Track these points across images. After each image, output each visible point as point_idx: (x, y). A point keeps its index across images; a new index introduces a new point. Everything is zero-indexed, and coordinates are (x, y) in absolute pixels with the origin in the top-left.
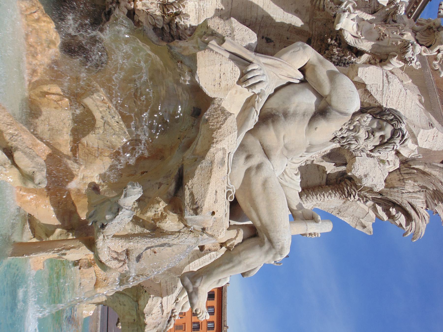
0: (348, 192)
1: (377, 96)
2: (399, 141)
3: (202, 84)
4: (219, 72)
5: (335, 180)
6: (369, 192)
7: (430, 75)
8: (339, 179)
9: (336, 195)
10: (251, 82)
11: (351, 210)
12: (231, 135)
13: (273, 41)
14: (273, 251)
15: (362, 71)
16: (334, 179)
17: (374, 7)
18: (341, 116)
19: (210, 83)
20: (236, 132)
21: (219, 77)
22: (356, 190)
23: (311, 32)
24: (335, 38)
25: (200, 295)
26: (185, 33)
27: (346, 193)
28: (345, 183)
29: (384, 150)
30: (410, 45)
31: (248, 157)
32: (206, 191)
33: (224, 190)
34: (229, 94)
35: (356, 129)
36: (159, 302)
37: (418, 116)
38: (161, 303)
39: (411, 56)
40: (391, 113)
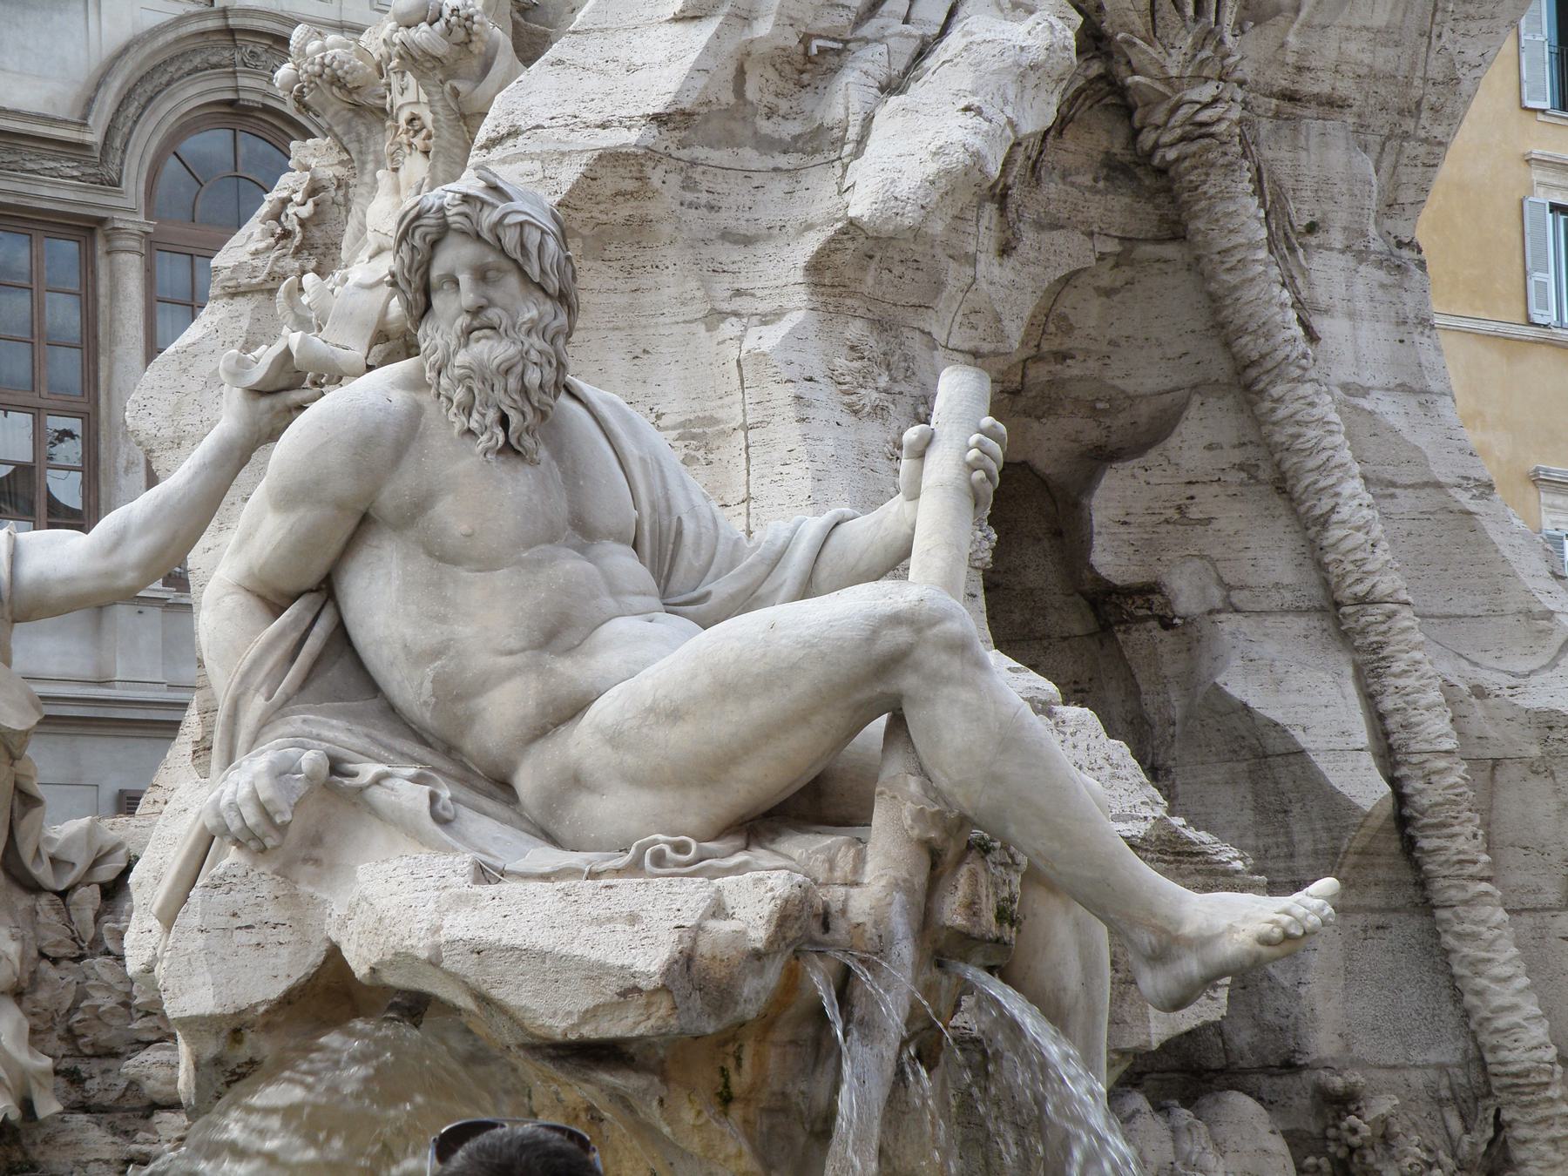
0: (1183, 139)
1: (562, 178)
2: (487, 211)
3: (276, 990)
6: (1166, 41)
16: (1157, 207)
17: (341, 163)
19: (273, 961)
22: (1165, 107)
25: (1205, 925)
27: (1193, 147)
31: (575, 781)
32: (579, 963)
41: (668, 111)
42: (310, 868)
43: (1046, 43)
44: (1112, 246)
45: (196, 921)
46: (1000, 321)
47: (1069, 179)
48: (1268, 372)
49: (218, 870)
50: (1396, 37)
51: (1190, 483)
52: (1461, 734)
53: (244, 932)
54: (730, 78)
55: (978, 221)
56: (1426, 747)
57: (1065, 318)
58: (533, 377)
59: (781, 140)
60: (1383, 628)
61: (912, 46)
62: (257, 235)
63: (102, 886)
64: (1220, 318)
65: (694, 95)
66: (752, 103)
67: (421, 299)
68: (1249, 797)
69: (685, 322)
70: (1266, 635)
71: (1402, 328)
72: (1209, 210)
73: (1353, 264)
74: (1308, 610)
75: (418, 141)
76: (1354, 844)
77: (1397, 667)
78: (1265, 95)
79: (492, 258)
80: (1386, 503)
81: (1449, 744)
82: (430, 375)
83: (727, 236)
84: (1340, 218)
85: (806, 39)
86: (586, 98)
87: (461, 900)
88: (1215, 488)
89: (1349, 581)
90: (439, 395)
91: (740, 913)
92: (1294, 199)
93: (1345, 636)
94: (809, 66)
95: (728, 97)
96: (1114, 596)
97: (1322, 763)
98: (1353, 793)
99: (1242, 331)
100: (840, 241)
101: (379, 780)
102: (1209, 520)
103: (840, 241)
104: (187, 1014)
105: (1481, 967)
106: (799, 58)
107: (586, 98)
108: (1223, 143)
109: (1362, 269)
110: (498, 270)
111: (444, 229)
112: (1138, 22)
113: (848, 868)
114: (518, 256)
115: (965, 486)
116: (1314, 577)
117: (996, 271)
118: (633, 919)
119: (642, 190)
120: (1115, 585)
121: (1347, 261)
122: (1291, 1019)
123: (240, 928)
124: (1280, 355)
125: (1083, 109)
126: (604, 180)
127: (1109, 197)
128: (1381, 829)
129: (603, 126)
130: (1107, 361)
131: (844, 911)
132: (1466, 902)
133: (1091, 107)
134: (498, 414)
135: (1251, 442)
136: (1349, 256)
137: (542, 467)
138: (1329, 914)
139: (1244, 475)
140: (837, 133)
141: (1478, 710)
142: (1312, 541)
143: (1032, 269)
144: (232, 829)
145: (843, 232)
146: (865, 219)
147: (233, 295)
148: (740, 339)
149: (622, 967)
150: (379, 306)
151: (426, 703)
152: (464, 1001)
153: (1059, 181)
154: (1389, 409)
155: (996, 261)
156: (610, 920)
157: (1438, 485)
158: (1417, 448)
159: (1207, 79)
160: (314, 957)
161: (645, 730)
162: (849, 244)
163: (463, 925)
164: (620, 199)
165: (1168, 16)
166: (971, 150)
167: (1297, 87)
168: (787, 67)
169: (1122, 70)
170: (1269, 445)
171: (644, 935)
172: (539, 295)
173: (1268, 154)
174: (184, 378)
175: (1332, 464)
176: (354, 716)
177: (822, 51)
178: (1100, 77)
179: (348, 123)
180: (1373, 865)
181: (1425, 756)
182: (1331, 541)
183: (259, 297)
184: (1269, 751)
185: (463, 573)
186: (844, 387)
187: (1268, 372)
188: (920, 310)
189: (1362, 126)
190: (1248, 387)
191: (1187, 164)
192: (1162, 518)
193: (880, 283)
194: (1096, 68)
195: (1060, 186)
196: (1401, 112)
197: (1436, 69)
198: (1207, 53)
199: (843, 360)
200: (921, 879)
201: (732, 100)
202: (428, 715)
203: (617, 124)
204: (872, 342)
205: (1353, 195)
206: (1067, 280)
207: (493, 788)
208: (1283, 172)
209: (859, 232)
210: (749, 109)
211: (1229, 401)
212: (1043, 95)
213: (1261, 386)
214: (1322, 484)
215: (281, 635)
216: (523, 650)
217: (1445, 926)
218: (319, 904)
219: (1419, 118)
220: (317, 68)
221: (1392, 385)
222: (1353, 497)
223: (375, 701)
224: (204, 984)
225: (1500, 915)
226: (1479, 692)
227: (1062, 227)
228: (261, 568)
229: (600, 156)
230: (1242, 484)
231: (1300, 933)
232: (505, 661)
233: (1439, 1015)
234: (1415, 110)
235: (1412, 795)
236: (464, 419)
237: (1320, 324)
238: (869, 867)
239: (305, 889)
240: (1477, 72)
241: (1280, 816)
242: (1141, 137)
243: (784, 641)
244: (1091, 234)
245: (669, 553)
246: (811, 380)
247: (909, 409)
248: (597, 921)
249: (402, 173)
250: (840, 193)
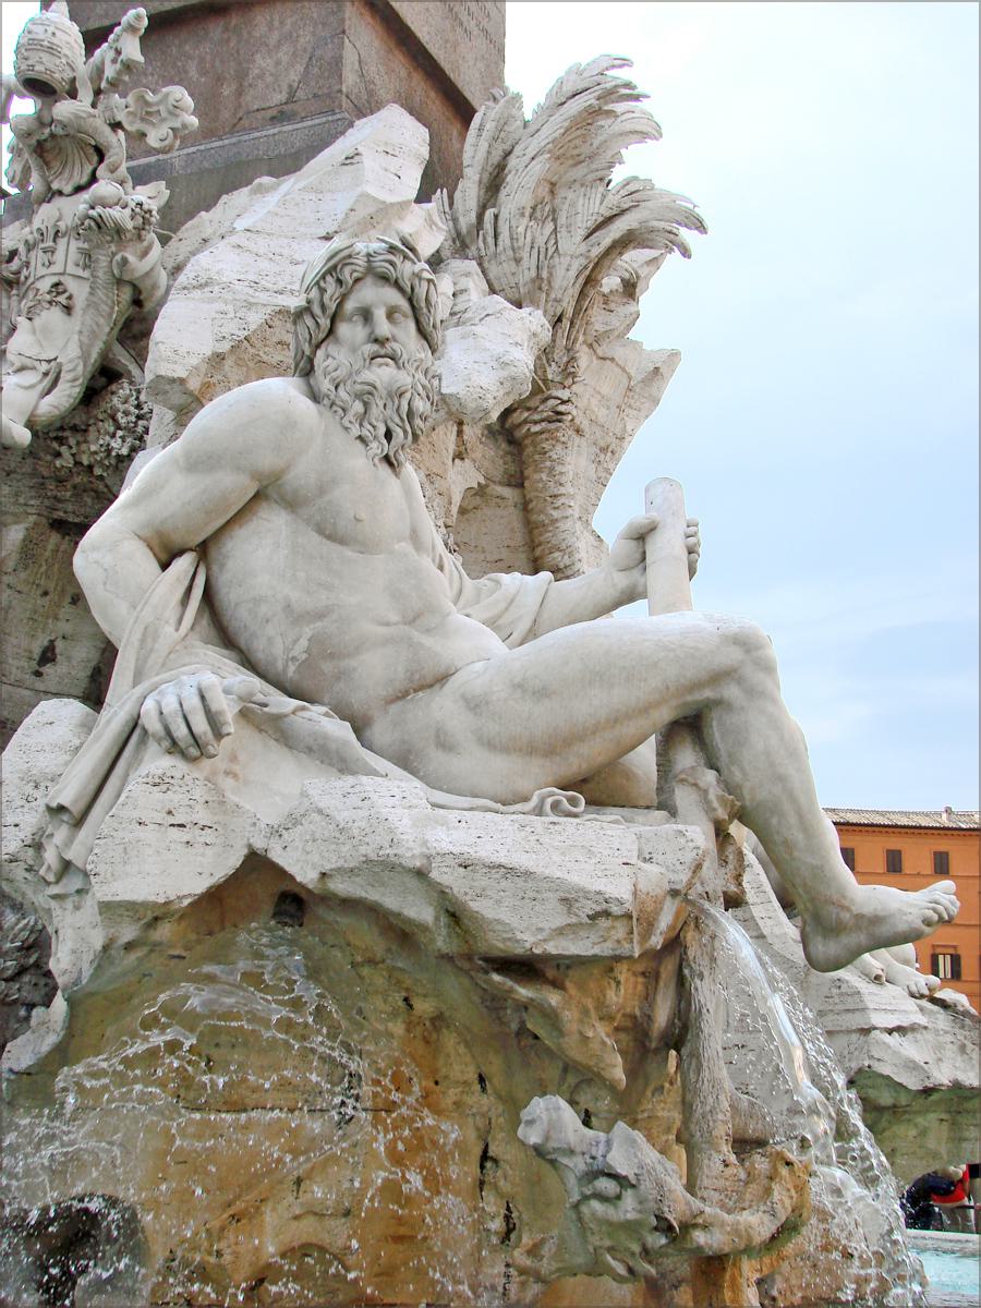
2: (408, 264)
3: (200, 886)
4: (163, 829)
7: (188, 154)
10: (201, 725)
11: (601, 414)
12: (374, 797)
13: (52, 642)
14: (749, 671)
15: (169, 366)
19: (200, 858)
20: (364, 779)
23: (32, 519)
24: (55, 445)
25: (879, 907)
26: (13, 929)
28: (520, 425)
29: (432, 311)
30: (92, 212)
32: (554, 884)
33: (551, 826)
34: (236, 799)
35: (366, 396)
36: (886, 1037)
37: (320, 196)
38: (890, 1031)
39: (128, 211)
40: (317, 283)
53: (176, 829)
67: (325, 322)
72: (552, 469)
75: (62, 299)
79: (404, 304)
104: (118, 899)
149: (599, 893)
160: (234, 861)
171: (604, 867)
185: (348, 553)
191: (543, 436)
218: (244, 813)
232: (382, 630)
239: (232, 797)
243: (647, 644)
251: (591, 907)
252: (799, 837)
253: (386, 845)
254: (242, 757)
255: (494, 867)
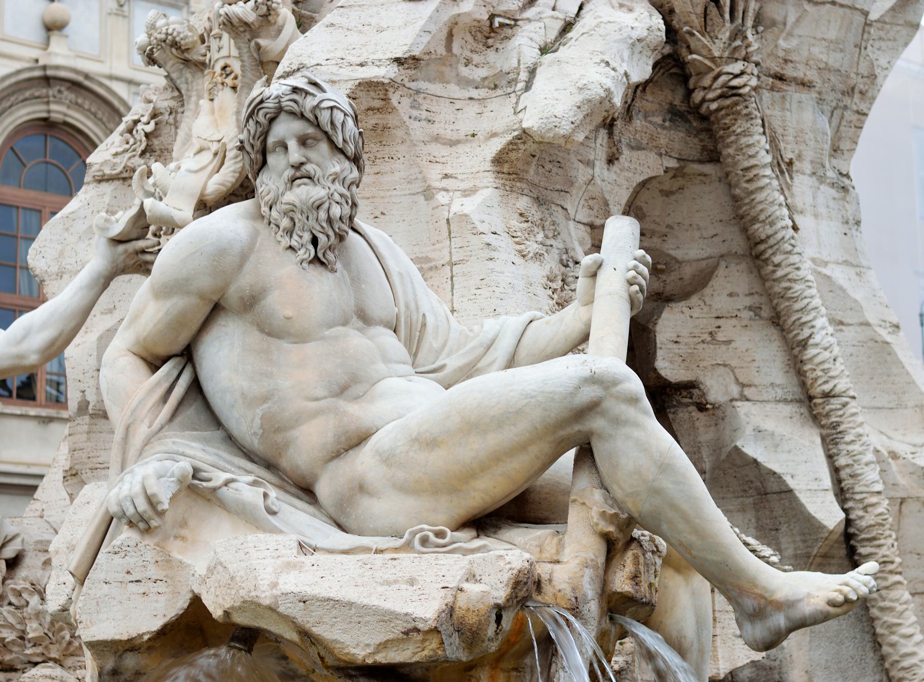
0: (722, 96)
2: (309, 98)
3: (156, 625)
4: (124, 585)
5: (703, 136)
6: (712, 34)
8: (695, 124)
9: (739, 130)
16: (701, 140)
17: (173, 98)
18: (253, 258)
21: (138, 583)
27: (728, 102)
31: (362, 488)
34: (180, 557)
41: (405, 56)
42: (178, 543)
43: (647, 26)
44: (673, 164)
45: (102, 576)
46: (608, 205)
47: (649, 119)
48: (771, 247)
49: (117, 542)
50: (841, 46)
51: (718, 317)
52: (884, 483)
53: (134, 584)
54: (444, 38)
55: (596, 140)
56: (865, 489)
57: (641, 209)
58: (336, 211)
59: (474, 80)
60: (840, 413)
61: (559, 25)
62: (117, 143)
63: (7, 561)
64: (741, 212)
65: (422, 47)
66: (456, 56)
67: (259, 157)
68: (753, 520)
69: (410, 194)
70: (767, 416)
71: (845, 226)
72: (735, 142)
73: (817, 184)
74: (791, 401)
75: (229, 81)
76: (821, 550)
77: (848, 438)
78: (766, 75)
79: (311, 130)
80: (839, 335)
81: (879, 487)
82: (264, 209)
83: (437, 139)
84: (809, 155)
85: (492, 17)
86: (350, 48)
87: (290, 566)
88: (734, 321)
89: (820, 382)
90: (270, 223)
91: (485, 578)
92: (783, 141)
93: (815, 418)
94: (492, 35)
95: (442, 51)
96: (668, 390)
97: (803, 498)
98: (822, 518)
99: (755, 220)
100: (516, 144)
101: (227, 483)
102: (729, 342)
103: (516, 144)
105: (894, 629)
106: (487, 29)
107: (350, 48)
108: (745, 100)
109: (822, 187)
110: (315, 139)
111: (280, 110)
112: (696, 21)
113: (554, 551)
114: (328, 128)
115: (626, 296)
116: (795, 380)
117: (606, 173)
118: (412, 582)
119: (386, 107)
120: (670, 382)
121: (813, 181)
122: (777, 663)
123: (132, 582)
124: (779, 236)
125: (659, 74)
126: (361, 99)
127: (672, 132)
128: (837, 541)
129: (362, 65)
130: (665, 238)
131: (550, 580)
132: (887, 588)
133: (663, 74)
134: (311, 237)
135: (757, 293)
136: (814, 178)
137: (338, 274)
138: (874, 586)
139: (752, 313)
140: (512, 76)
141: (894, 465)
142: (796, 357)
143: (626, 174)
144: (128, 514)
145: (519, 138)
146: (535, 129)
147: (100, 181)
148: (449, 205)
149: (406, 614)
150: (201, 185)
151: (255, 434)
152: (291, 635)
153: (643, 120)
154: (839, 274)
155: (606, 166)
156: (396, 582)
157: (867, 324)
158: (856, 301)
159: (737, 60)
160: (181, 604)
161: (411, 454)
162: (522, 147)
163: (292, 583)
164: (370, 112)
165: (715, 18)
166: (604, 87)
167: (784, 72)
168: (479, 34)
169: (684, 51)
170: (770, 295)
171: (421, 592)
172: (342, 157)
173: (768, 112)
174: (66, 235)
175: (810, 307)
176: (206, 441)
177: (502, 25)
178: (669, 56)
179: (181, 70)
180: (829, 564)
181: (864, 495)
182: (809, 356)
183: (117, 183)
184: (769, 491)
185: (285, 345)
186: (516, 240)
187: (771, 247)
188: (562, 193)
189: (821, 99)
190: (758, 257)
191: (723, 112)
192: (700, 340)
193: (537, 174)
194: (668, 50)
195: (643, 123)
196: (843, 93)
197: (863, 69)
198: (738, 43)
199: (515, 222)
200: (601, 560)
201: (444, 53)
202: (256, 442)
203: (371, 64)
204: (533, 212)
205: (817, 141)
206: (643, 184)
207: (300, 493)
208: (776, 123)
209: (529, 138)
210: (454, 59)
211: (743, 266)
212: (644, 58)
213: (767, 255)
214: (804, 319)
215: (158, 384)
216: (325, 398)
217: (873, 603)
218: (186, 567)
219: (853, 97)
220: (163, 36)
221: (840, 261)
222: (823, 328)
223: (219, 432)
224: (108, 619)
225: (907, 596)
226: (894, 456)
227: (644, 149)
228: (145, 339)
229: (360, 83)
230: (751, 319)
231: (855, 598)
233: (865, 659)
234: (850, 92)
235: (855, 520)
236: (287, 239)
237: (799, 220)
238: (567, 551)
239: (176, 555)
240: (885, 72)
241: (773, 533)
242: (694, 95)
244: (661, 155)
245: (417, 338)
246: (495, 233)
247: (557, 257)
248: (388, 583)
249: (216, 101)
250: (515, 113)
251: (402, 626)
252: (693, 538)
253: (253, 589)
254: (191, 523)
255: (325, 601)
